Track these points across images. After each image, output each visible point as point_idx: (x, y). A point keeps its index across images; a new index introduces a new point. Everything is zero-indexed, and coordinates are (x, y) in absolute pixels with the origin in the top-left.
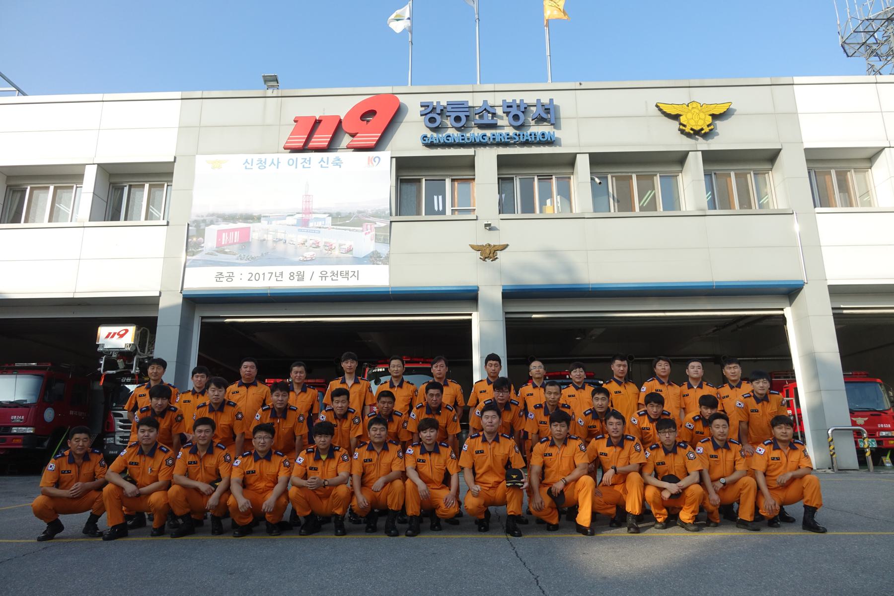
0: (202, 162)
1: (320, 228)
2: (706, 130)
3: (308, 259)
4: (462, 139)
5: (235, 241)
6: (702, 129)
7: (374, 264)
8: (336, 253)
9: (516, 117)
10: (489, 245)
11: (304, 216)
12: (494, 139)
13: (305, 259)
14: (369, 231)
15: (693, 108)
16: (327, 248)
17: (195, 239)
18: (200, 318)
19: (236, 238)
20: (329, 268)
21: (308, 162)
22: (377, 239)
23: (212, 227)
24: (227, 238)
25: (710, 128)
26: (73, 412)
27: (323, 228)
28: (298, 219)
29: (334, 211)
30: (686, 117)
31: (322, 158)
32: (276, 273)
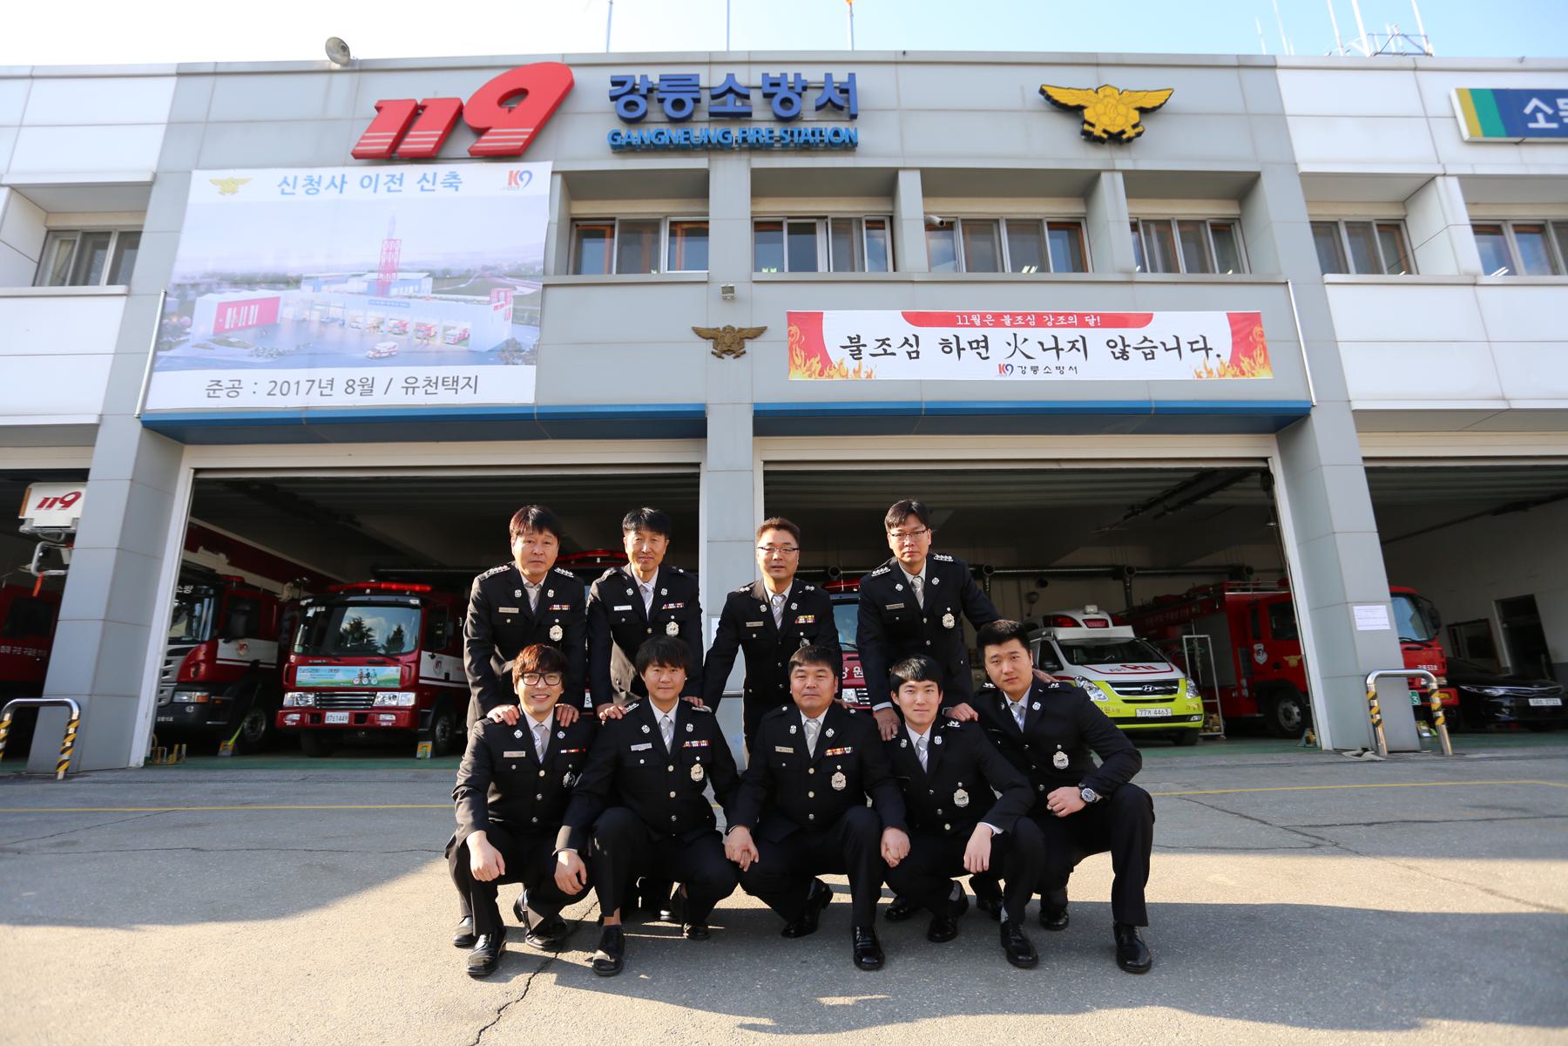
0: (203, 186)
1: (410, 297)
2: (1131, 133)
3: (383, 355)
4: (686, 139)
5: (250, 323)
6: (1123, 132)
7: (507, 364)
8: (437, 342)
9: (786, 102)
10: (733, 329)
11: (381, 275)
12: (744, 140)
13: (377, 355)
14: (503, 302)
15: (1105, 96)
16: (420, 334)
17: (175, 320)
18: (192, 471)
19: (251, 318)
20: (421, 372)
21: (398, 182)
22: (517, 318)
23: (209, 296)
24: (235, 316)
25: (1137, 130)
26: (9, 648)
27: (416, 297)
28: (369, 282)
29: (440, 264)
30: (1094, 110)
31: (425, 175)
32: (320, 380)
